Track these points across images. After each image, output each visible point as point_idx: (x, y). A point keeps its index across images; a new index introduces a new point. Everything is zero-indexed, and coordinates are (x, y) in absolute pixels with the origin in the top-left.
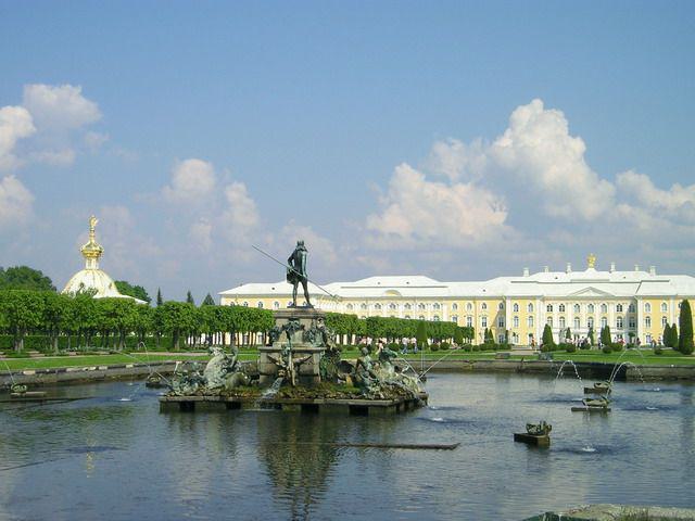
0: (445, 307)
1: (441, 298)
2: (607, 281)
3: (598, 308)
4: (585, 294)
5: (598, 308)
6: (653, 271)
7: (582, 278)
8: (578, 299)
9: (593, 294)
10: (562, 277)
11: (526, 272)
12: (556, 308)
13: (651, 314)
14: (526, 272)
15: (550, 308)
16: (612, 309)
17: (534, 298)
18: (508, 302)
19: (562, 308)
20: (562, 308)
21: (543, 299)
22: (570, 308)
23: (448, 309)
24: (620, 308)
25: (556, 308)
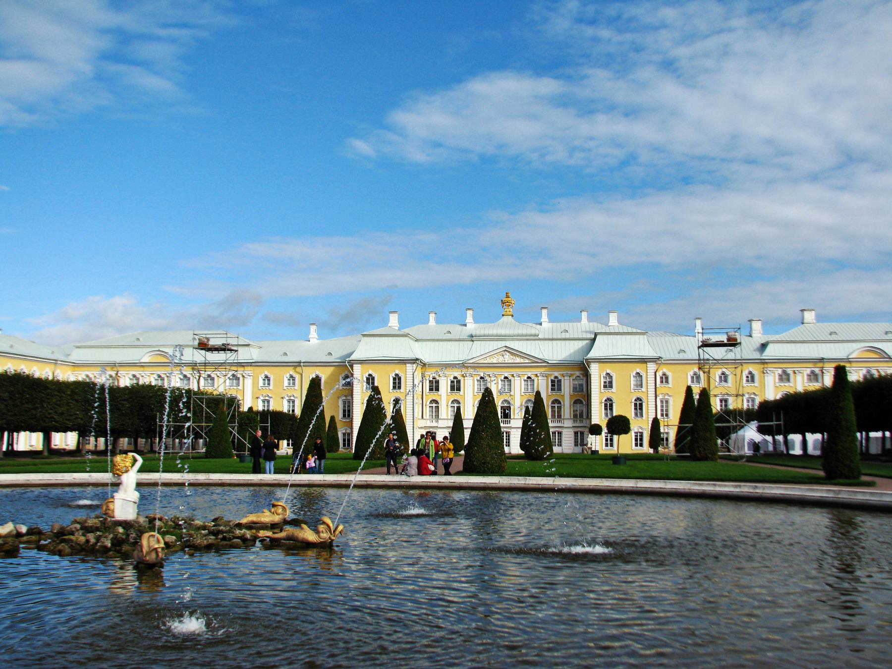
0: (249, 382)
2: (534, 338)
6: (613, 319)
7: (495, 332)
9: (508, 359)
10: (457, 330)
11: (394, 321)
12: (445, 385)
13: (612, 393)
14: (394, 321)
15: (435, 386)
17: (403, 362)
19: (456, 386)
20: (456, 386)
23: (255, 383)
25: (445, 385)
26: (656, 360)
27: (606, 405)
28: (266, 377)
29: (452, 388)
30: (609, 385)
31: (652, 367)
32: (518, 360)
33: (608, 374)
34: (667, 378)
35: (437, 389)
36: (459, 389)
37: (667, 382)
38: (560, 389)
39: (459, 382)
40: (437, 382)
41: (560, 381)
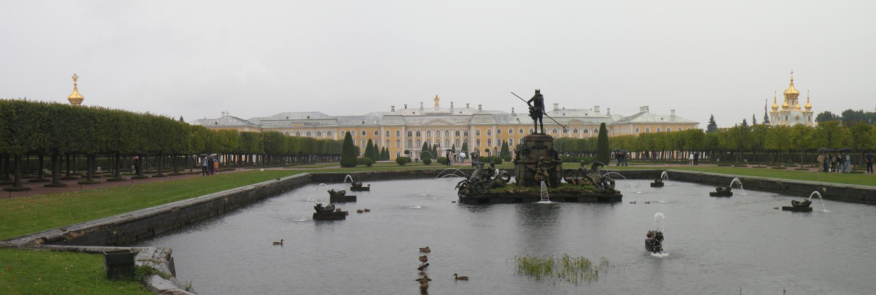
1: (333, 127)
3: (443, 134)
4: (434, 124)
5: (443, 134)
8: (431, 127)
9: (438, 123)
12: (414, 134)
13: (480, 137)
15: (410, 134)
16: (452, 134)
18: (382, 129)
19: (418, 134)
21: (406, 127)
22: (424, 134)
24: (458, 133)
25: (414, 134)
26: (497, 125)
27: (477, 142)
28: (343, 132)
29: (417, 135)
30: (478, 134)
31: (494, 128)
32: (443, 124)
33: (478, 130)
34: (500, 131)
35: (411, 135)
36: (420, 135)
37: (500, 132)
38: (459, 135)
39: (420, 132)
40: (411, 132)
41: (459, 132)
